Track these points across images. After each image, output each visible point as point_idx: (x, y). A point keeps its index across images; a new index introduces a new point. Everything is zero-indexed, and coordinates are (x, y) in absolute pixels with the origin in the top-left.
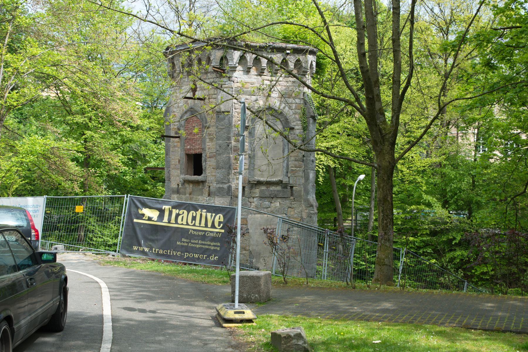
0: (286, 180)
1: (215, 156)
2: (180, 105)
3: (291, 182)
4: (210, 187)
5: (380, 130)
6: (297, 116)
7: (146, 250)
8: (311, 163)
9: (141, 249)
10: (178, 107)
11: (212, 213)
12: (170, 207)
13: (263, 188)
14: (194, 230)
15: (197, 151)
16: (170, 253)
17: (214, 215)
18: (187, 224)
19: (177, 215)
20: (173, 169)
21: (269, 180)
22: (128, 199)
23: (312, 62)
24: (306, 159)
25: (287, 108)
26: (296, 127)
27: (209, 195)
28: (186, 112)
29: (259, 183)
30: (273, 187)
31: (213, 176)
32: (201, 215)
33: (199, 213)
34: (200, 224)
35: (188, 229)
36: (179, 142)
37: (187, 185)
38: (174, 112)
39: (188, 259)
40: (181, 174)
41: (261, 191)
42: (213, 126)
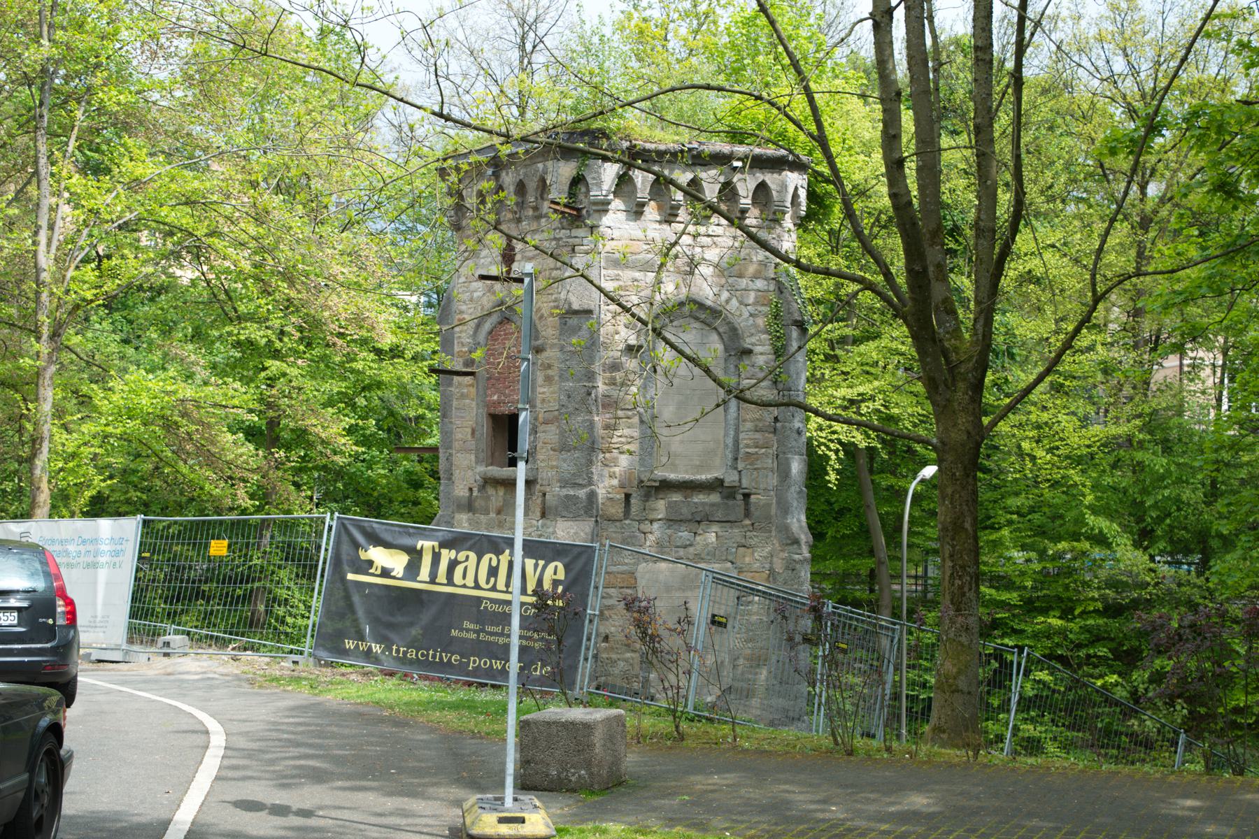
0: (731, 478)
1: (556, 419)
2: (475, 295)
3: (745, 483)
4: (544, 495)
5: (945, 353)
6: (761, 322)
7: (377, 648)
8: (795, 436)
9: (363, 647)
10: (471, 300)
11: (537, 558)
12: (436, 544)
13: (676, 497)
14: (493, 601)
16: (434, 656)
17: (541, 563)
18: (477, 586)
19: (453, 565)
21: (687, 477)
22: (334, 524)
23: (796, 189)
24: (783, 427)
25: (734, 302)
26: (758, 349)
27: (543, 515)
29: (666, 486)
30: (701, 496)
31: (552, 467)
32: (511, 564)
33: (505, 558)
34: (508, 585)
35: (479, 600)
36: (472, 385)
37: (491, 491)
38: (461, 312)
39: (477, 672)
40: (477, 463)
41: (670, 506)
42: (553, 346)
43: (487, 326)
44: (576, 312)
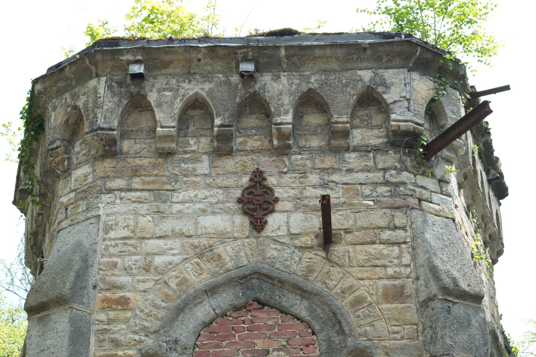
44: (464, 295)
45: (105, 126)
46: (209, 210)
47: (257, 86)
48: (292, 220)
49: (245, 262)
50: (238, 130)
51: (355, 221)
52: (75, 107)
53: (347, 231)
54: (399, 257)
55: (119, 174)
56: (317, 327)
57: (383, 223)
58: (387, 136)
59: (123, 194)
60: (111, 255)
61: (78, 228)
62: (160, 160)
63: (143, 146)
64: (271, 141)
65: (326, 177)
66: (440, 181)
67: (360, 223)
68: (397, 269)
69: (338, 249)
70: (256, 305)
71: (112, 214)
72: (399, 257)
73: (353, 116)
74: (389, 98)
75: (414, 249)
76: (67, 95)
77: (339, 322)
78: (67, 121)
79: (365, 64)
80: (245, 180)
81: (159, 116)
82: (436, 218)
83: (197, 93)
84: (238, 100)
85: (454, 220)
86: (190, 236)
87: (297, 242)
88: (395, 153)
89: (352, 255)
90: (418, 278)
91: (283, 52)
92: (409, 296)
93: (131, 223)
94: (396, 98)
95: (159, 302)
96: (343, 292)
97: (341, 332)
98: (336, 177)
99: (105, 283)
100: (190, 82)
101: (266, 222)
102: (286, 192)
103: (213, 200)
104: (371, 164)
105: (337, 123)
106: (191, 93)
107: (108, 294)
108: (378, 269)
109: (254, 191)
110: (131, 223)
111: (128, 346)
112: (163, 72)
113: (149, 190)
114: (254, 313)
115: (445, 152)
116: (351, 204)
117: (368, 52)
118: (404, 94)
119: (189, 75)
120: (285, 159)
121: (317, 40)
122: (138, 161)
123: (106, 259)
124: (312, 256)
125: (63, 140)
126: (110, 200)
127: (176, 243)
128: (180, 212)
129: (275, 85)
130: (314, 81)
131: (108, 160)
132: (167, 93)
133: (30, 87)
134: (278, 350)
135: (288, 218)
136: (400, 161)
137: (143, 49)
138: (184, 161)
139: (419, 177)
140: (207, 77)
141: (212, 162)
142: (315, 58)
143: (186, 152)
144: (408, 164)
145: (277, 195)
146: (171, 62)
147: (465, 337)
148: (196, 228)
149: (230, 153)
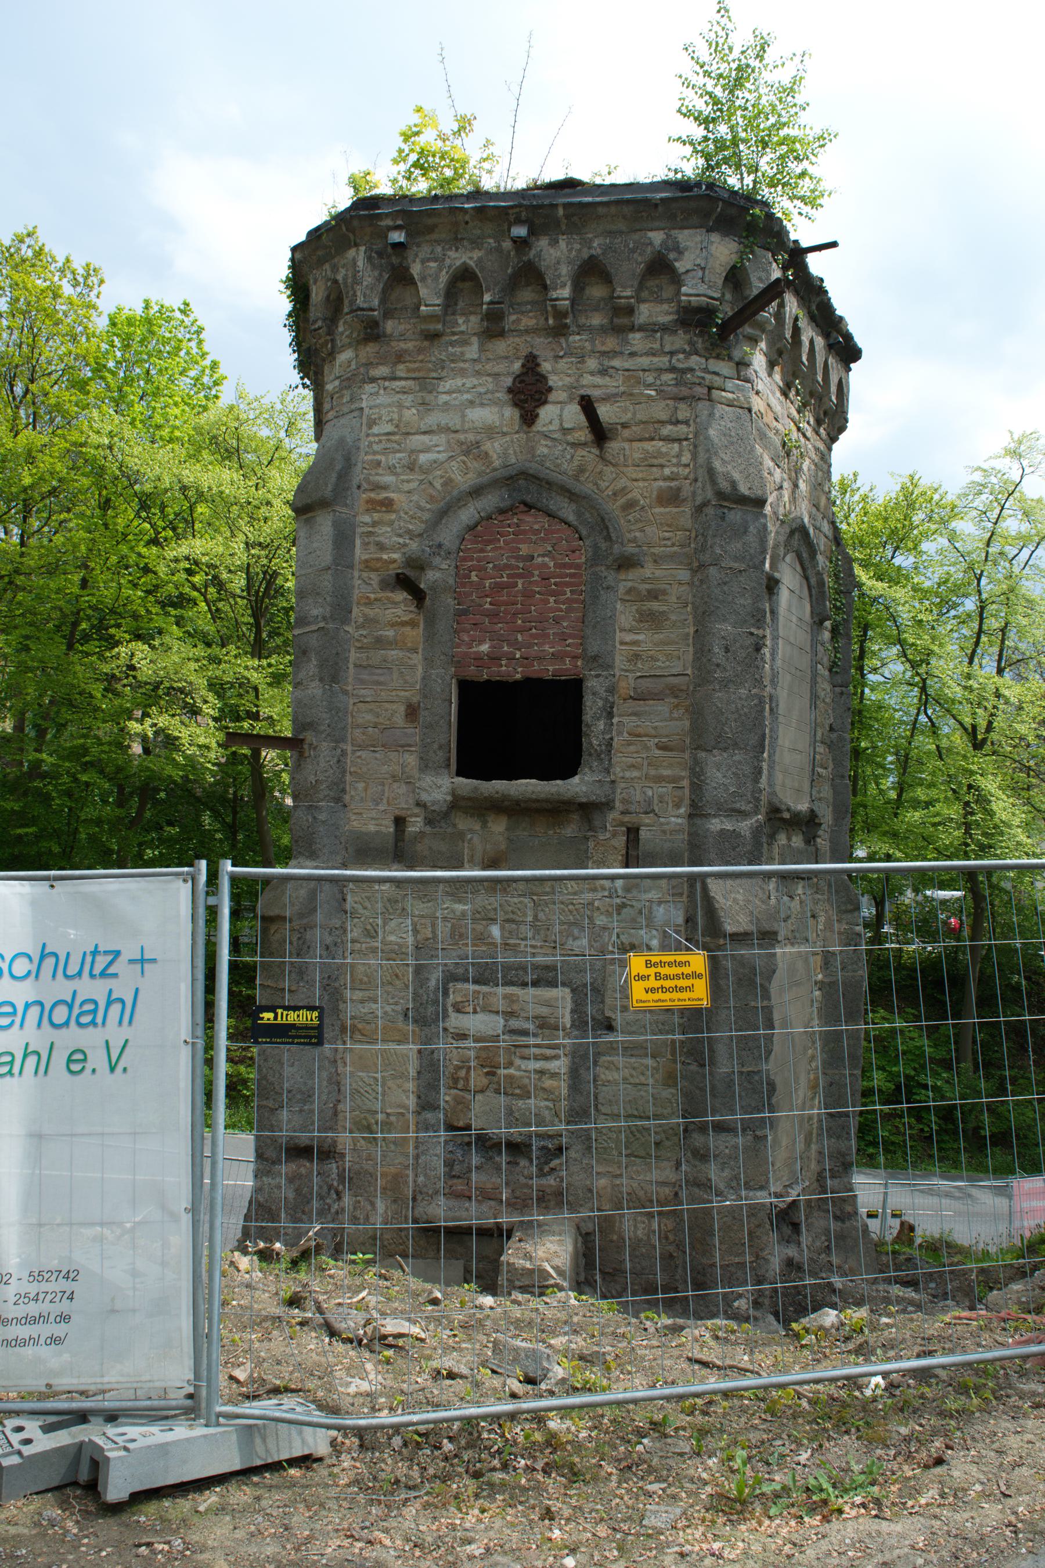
2: (423, 458)
15: (549, 670)
20: (361, 747)
28: (476, 492)
37: (464, 823)
40: (425, 766)
43: (467, 515)
44: (743, 500)
45: (365, 306)
46: (477, 401)
47: (532, 253)
48: (566, 413)
49: (513, 461)
50: (511, 306)
51: (634, 414)
52: (336, 282)
53: (624, 426)
54: (678, 456)
55: (382, 361)
56: (584, 532)
57: (664, 417)
58: (678, 312)
59: (387, 384)
60: (375, 453)
61: (343, 421)
62: (426, 343)
63: (408, 327)
64: (547, 319)
65: (606, 363)
66: (738, 364)
67: (639, 417)
68: (675, 469)
69: (613, 446)
70: (522, 508)
71: (376, 406)
72: (678, 456)
73: (641, 287)
74: (681, 266)
75: (695, 447)
76: (327, 266)
77: (607, 528)
78: (328, 297)
79: (657, 224)
80: (517, 366)
81: (423, 292)
82: (727, 408)
83: (464, 263)
84: (509, 271)
85: (750, 410)
86: (456, 432)
87: (569, 438)
88: (685, 333)
89: (627, 453)
90: (696, 480)
91: (561, 212)
92: (684, 500)
93: (396, 416)
94: (689, 267)
95: (423, 504)
96: (615, 494)
97: (608, 538)
98: (616, 363)
99: (369, 482)
100: (457, 249)
101: (537, 415)
102: (561, 379)
103: (482, 390)
104: (657, 346)
105: (619, 297)
106: (458, 263)
107: (372, 495)
108: (654, 469)
109: (526, 378)
110: (396, 416)
111: (393, 549)
112: (427, 238)
113: (414, 379)
114: (521, 516)
115: (748, 329)
116: (631, 395)
117: (660, 209)
118: (698, 261)
119: (456, 241)
120: (563, 340)
121: (602, 194)
122: (403, 345)
123: (370, 457)
124: (584, 453)
125: (324, 320)
126: (373, 391)
127: (441, 439)
128: (446, 403)
129: (552, 251)
130: (597, 245)
131: (371, 344)
132: (433, 264)
133: (289, 255)
134: (543, 556)
135: (562, 410)
136: (691, 343)
137: (403, 212)
138: (452, 344)
139: (711, 361)
140: (476, 243)
141: (481, 345)
142: (599, 217)
143: (454, 334)
144: (699, 346)
145: (551, 383)
146: (435, 226)
147: (739, 546)
148: (463, 421)
149: (501, 334)
